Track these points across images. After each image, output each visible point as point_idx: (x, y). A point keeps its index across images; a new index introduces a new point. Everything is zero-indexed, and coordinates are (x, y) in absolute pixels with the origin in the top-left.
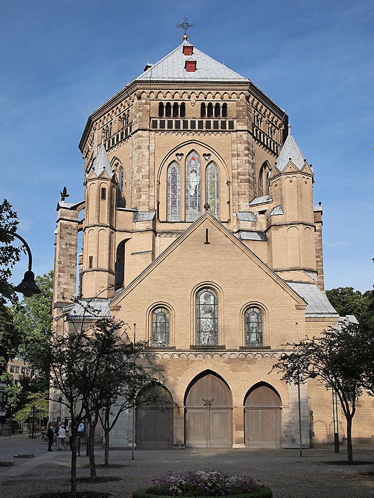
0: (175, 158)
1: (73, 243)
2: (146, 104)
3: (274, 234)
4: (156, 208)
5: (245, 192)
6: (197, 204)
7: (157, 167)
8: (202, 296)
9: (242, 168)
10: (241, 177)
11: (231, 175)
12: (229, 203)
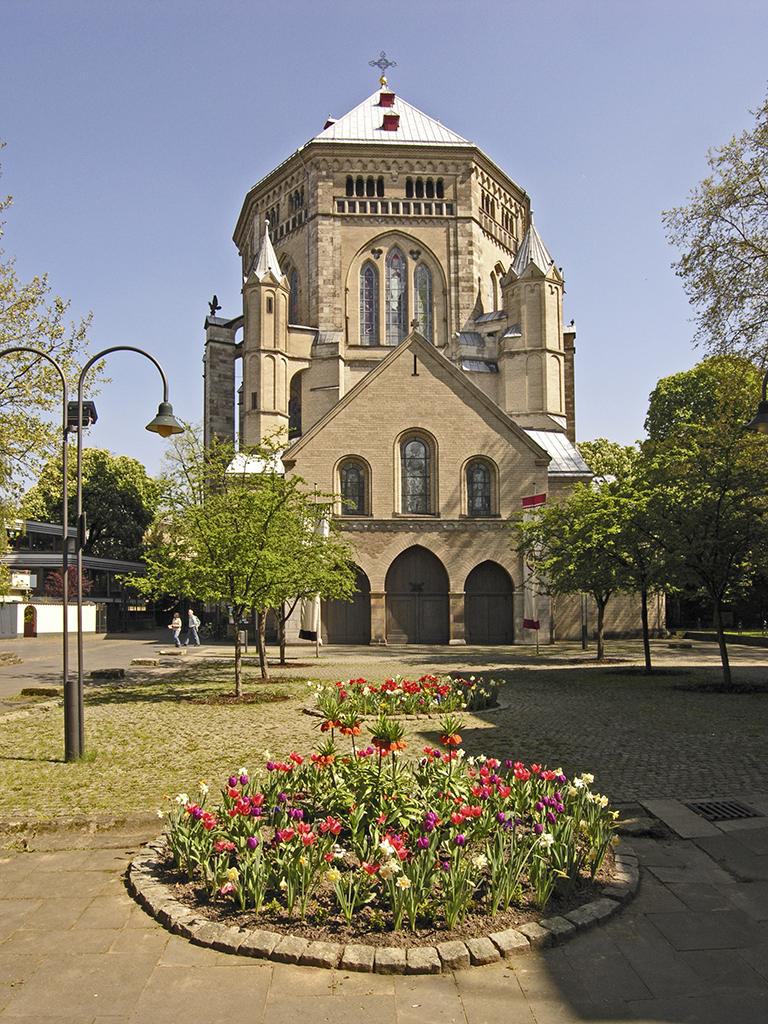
0: (372, 257)
3: (506, 365)
8: (409, 448)
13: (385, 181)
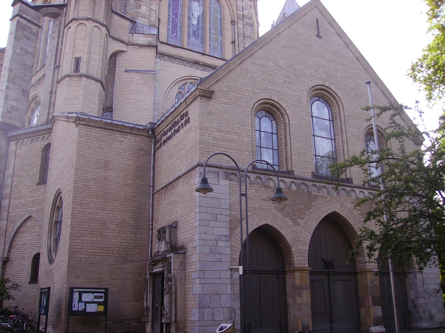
1: (31, 50)
4: (157, 25)
9: (247, 11)
10: (246, 20)
11: (235, 15)
12: (233, 42)
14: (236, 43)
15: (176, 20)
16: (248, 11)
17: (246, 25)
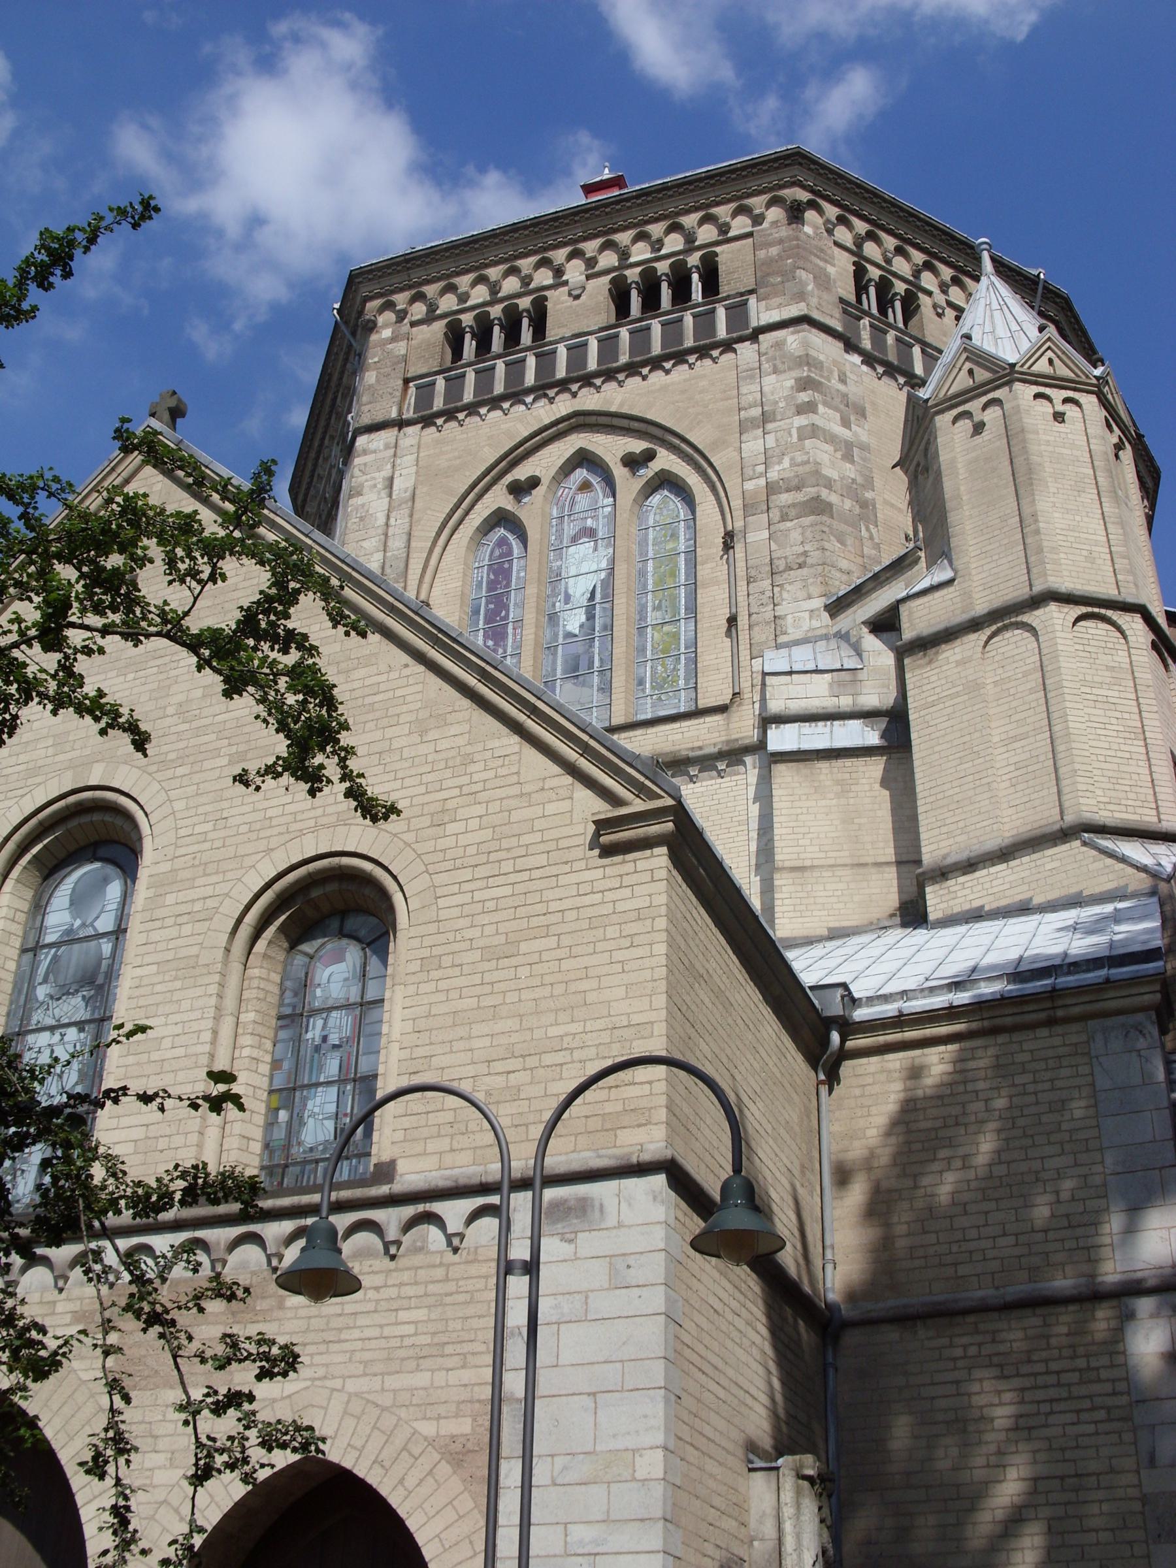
2: (394, 339)
5: (805, 553)
6: (597, 663)
7: (421, 545)
10: (785, 498)
12: (732, 621)
13: (549, 305)
14: (743, 621)
15: (500, 651)
16: (792, 459)
17: (784, 518)
